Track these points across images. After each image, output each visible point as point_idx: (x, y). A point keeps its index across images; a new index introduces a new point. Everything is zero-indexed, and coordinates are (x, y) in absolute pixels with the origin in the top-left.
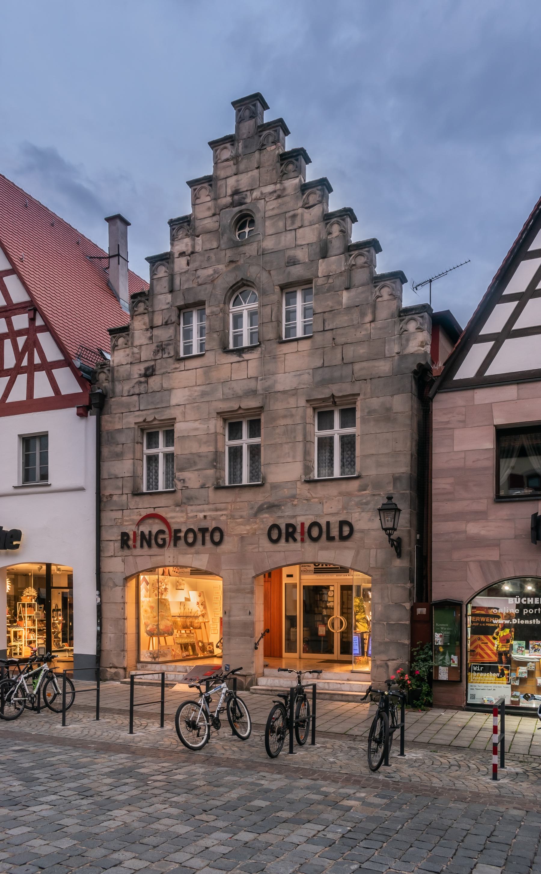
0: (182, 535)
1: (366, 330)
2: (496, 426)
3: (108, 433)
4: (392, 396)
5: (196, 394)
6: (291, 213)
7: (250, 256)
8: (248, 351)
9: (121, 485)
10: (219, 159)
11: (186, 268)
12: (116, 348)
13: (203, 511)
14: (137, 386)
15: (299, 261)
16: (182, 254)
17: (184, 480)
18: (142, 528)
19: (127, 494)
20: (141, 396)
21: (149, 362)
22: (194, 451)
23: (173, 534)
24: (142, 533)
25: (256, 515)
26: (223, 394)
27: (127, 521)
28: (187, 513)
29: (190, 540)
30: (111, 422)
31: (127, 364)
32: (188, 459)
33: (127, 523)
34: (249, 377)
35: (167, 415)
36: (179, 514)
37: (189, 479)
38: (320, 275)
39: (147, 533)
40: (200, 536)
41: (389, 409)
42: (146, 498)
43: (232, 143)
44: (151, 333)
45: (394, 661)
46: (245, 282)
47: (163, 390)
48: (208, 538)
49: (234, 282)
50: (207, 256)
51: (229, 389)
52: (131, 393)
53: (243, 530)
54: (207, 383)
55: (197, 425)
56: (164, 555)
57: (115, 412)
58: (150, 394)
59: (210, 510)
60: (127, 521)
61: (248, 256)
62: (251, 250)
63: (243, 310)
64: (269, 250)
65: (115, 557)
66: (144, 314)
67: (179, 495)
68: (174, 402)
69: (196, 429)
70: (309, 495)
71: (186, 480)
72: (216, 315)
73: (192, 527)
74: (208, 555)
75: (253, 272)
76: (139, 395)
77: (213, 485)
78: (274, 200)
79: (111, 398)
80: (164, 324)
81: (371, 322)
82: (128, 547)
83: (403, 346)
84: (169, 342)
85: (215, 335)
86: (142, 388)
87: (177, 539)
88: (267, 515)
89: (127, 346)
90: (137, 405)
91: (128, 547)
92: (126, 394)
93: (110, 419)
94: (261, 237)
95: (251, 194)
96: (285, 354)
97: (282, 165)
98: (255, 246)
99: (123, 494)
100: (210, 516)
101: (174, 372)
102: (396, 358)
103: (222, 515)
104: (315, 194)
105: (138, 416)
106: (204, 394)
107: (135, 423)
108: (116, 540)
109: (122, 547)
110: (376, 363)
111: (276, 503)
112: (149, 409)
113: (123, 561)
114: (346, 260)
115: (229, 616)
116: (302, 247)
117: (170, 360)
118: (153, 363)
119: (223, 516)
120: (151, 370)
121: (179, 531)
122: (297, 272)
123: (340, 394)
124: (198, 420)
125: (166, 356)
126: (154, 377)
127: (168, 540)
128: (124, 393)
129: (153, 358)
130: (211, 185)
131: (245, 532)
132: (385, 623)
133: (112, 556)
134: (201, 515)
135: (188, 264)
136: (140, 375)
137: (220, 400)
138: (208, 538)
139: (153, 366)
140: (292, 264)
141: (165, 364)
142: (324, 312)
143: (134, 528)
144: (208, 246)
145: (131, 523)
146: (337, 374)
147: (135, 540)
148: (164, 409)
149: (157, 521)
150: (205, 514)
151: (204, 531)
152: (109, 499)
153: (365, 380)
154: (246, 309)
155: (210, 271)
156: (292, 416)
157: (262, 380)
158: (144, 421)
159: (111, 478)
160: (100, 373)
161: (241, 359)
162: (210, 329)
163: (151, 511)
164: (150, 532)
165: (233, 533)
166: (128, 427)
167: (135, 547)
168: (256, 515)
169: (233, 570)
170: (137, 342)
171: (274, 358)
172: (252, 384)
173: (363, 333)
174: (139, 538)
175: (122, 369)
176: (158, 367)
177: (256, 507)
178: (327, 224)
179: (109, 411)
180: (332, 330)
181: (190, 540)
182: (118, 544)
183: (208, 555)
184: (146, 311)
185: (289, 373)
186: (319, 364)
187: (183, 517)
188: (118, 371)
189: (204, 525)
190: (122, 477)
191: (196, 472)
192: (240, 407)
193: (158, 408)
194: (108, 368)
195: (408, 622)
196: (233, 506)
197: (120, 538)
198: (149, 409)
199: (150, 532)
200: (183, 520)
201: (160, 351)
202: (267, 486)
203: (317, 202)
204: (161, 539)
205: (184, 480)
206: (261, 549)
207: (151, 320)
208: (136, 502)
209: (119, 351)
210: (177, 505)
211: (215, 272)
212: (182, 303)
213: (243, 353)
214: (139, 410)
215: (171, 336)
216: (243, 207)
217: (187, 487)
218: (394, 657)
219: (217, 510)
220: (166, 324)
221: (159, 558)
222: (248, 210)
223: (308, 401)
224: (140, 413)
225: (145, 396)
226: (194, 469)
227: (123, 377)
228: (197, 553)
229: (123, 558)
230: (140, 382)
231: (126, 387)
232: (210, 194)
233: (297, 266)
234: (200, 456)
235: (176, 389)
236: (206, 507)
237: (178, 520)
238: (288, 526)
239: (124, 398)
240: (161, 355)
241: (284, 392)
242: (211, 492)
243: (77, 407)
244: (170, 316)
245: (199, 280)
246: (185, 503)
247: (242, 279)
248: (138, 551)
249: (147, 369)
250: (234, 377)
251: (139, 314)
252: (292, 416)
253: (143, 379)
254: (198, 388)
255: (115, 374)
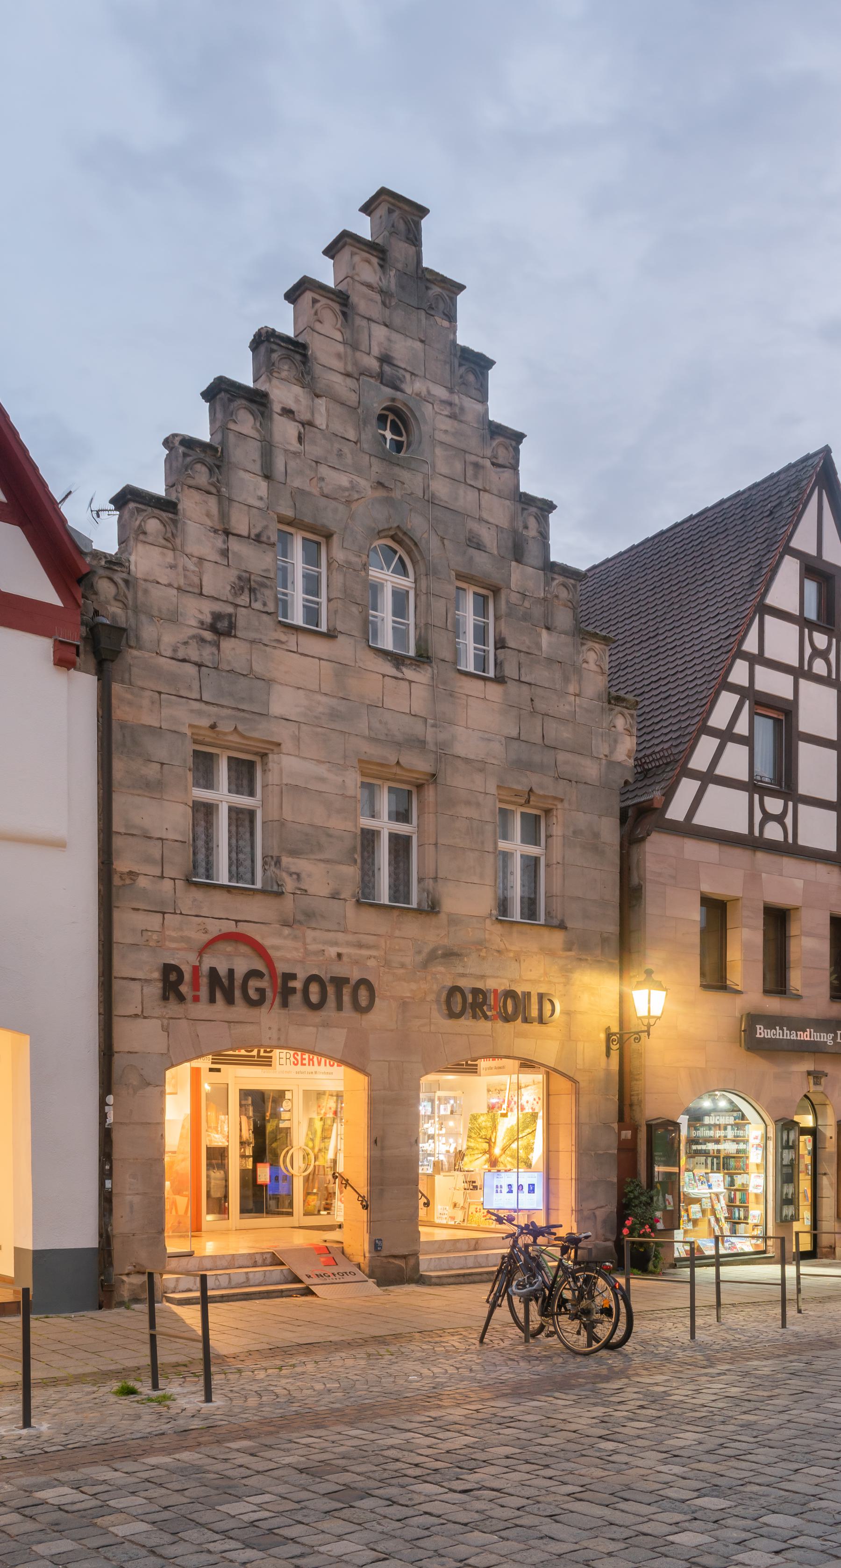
0: (298, 984)
1: (570, 704)
2: (702, 893)
3: (123, 726)
4: (600, 816)
5: (321, 709)
6: (473, 458)
7: (412, 493)
8: (411, 664)
9: (158, 856)
10: (358, 275)
11: (295, 446)
12: (141, 537)
13: (336, 944)
14: (193, 643)
15: (485, 547)
16: (288, 412)
17: (298, 875)
18: (208, 962)
19: (174, 879)
20: (203, 669)
21: (221, 603)
22: (318, 822)
23: (279, 981)
24: (213, 971)
25: (425, 964)
26: (370, 728)
27: (173, 940)
28: (305, 944)
29: (314, 998)
30: (130, 704)
31: (170, 585)
32: (307, 835)
33: (173, 945)
34: (413, 713)
35: (262, 731)
36: (289, 943)
37: (309, 876)
38: (513, 586)
39: (222, 971)
40: (331, 990)
41: (596, 835)
42: (219, 897)
43: (381, 263)
44: (224, 542)
45: (603, 1209)
46: (400, 535)
47: (250, 675)
48: (346, 998)
49: (386, 527)
50: (337, 446)
51: (380, 722)
52: (181, 655)
53: (406, 989)
54: (341, 695)
55: (322, 770)
56: (259, 1023)
57: (140, 683)
58: (224, 674)
59: (348, 944)
60: (173, 940)
61: (409, 492)
62: (413, 481)
63: (386, 581)
64: (441, 500)
65: (145, 1018)
66: (209, 493)
67: (288, 903)
68: (276, 708)
69: (322, 780)
70: (502, 946)
71: (303, 875)
72: (355, 570)
73: (315, 972)
74: (346, 1030)
75: (417, 524)
76: (200, 665)
77: (353, 896)
78: (447, 416)
79: (131, 647)
80: (253, 536)
81: (576, 695)
82: (181, 998)
83: (612, 751)
84: (265, 580)
85: (355, 610)
86: (207, 654)
87: (286, 993)
88: (441, 969)
89: (169, 545)
90: (196, 684)
91: (181, 998)
92: (169, 653)
93: (129, 696)
94: (426, 468)
95: (412, 382)
96: (467, 695)
97: (460, 365)
98: (419, 479)
99: (162, 877)
100: (349, 956)
101: (275, 647)
102: (604, 762)
103: (370, 957)
104: (507, 449)
105: (200, 713)
106: (334, 715)
107: (191, 726)
108: (146, 980)
109: (165, 998)
110: (577, 759)
111: (456, 949)
112: (222, 706)
113: (165, 1029)
114: (547, 583)
115: (382, 1148)
116: (489, 526)
117: (265, 618)
118: (230, 609)
119: (372, 959)
120: (226, 623)
121: (293, 977)
122: (482, 563)
123: (541, 793)
124: (324, 762)
125: (257, 605)
126: (233, 639)
127: (269, 994)
128: (162, 648)
129: (231, 599)
130: (344, 314)
131: (409, 995)
132: (593, 1153)
133: (136, 1016)
134: (333, 951)
135: (300, 439)
136: (202, 623)
137: (364, 737)
138: (346, 998)
139: (230, 615)
140: (475, 546)
141: (257, 624)
142: (520, 651)
143: (193, 958)
144: (338, 427)
145: (183, 945)
146: (537, 758)
147: (196, 986)
148: (257, 717)
149: (244, 949)
150: (340, 950)
151: (339, 982)
152: (128, 882)
153: (570, 781)
154: (392, 582)
155: (344, 480)
156: (478, 805)
157: (434, 726)
158: (213, 727)
159: (133, 835)
160: (101, 577)
161: (400, 675)
162: (345, 591)
163: (230, 927)
164: (231, 972)
165: (388, 994)
166: (174, 728)
167: (196, 999)
168: (425, 964)
169: (389, 1062)
170: (193, 548)
171: (451, 695)
172: (418, 729)
173: (567, 707)
174: (204, 981)
175: (157, 593)
176: (241, 623)
177: (426, 950)
178: (523, 509)
179: (127, 676)
180: (530, 684)
181: (314, 998)
182: (156, 989)
183: (346, 1030)
184: (214, 490)
185: (473, 730)
186: (514, 733)
187: (296, 949)
188: (146, 591)
189: (340, 970)
190: (161, 839)
191: (322, 865)
192: (398, 763)
193: (243, 711)
194: (124, 575)
195: (616, 1152)
196: (388, 942)
197: (156, 975)
198: (222, 706)
199: (231, 972)
200: (297, 955)
201: (246, 591)
202: (443, 917)
203: (508, 465)
204: (257, 990)
205: (298, 875)
206: (433, 1028)
207: (224, 516)
208: (195, 900)
209: (148, 547)
210: (285, 924)
211: (353, 487)
212: (289, 513)
213: (403, 664)
214: (200, 700)
215: (267, 570)
216: (398, 394)
217: (306, 891)
218: (602, 1204)
219: (360, 946)
220: (258, 539)
221: (249, 1029)
222: (405, 404)
223: (498, 786)
224: (203, 706)
225: (213, 673)
226: (318, 857)
227: (160, 611)
228: (326, 1025)
229: (165, 1022)
230: (203, 640)
231: (169, 638)
232: (343, 330)
233: (483, 554)
234: (329, 836)
235: (281, 684)
236: (340, 936)
237: (289, 956)
238: (476, 991)
239: (162, 660)
240: (248, 600)
241: (466, 760)
242: (350, 908)
243: (55, 640)
244: (266, 527)
245: (323, 484)
246: (300, 922)
247: (398, 527)
248: (202, 1009)
249: (217, 617)
250: (388, 703)
251: (198, 489)
252: (478, 805)
253: (208, 635)
254: (324, 699)
255: (140, 594)
